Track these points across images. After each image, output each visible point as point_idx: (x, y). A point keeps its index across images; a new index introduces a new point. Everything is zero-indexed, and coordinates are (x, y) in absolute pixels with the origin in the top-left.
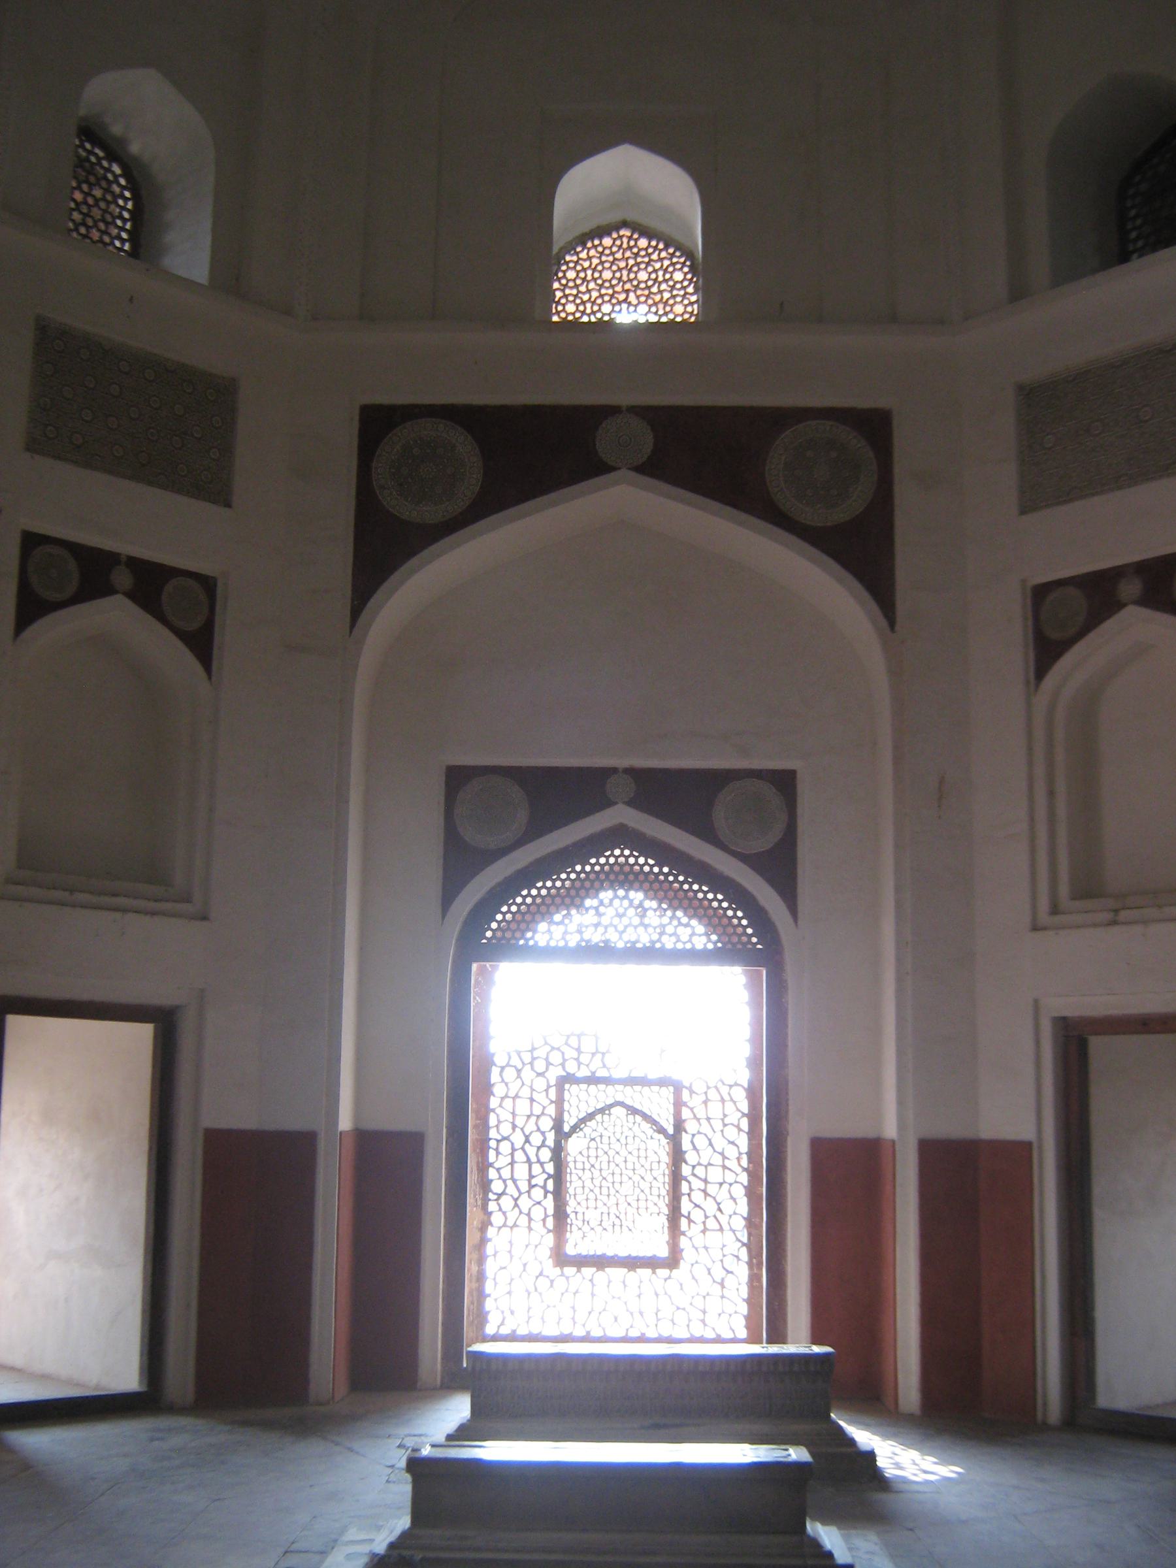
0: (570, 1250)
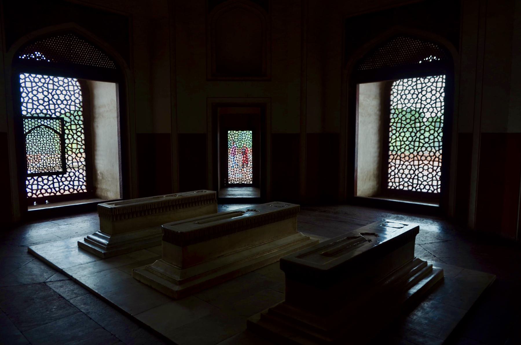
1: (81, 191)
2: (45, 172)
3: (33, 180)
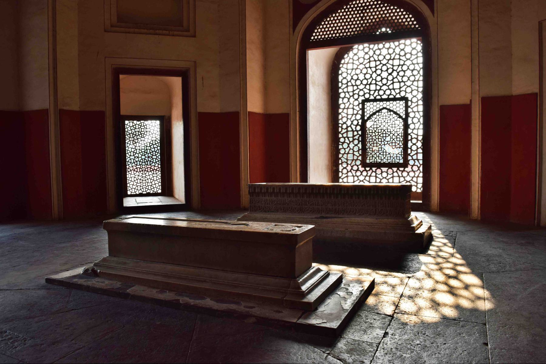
0: (368, 161)
2: (384, 163)
3: (371, 171)
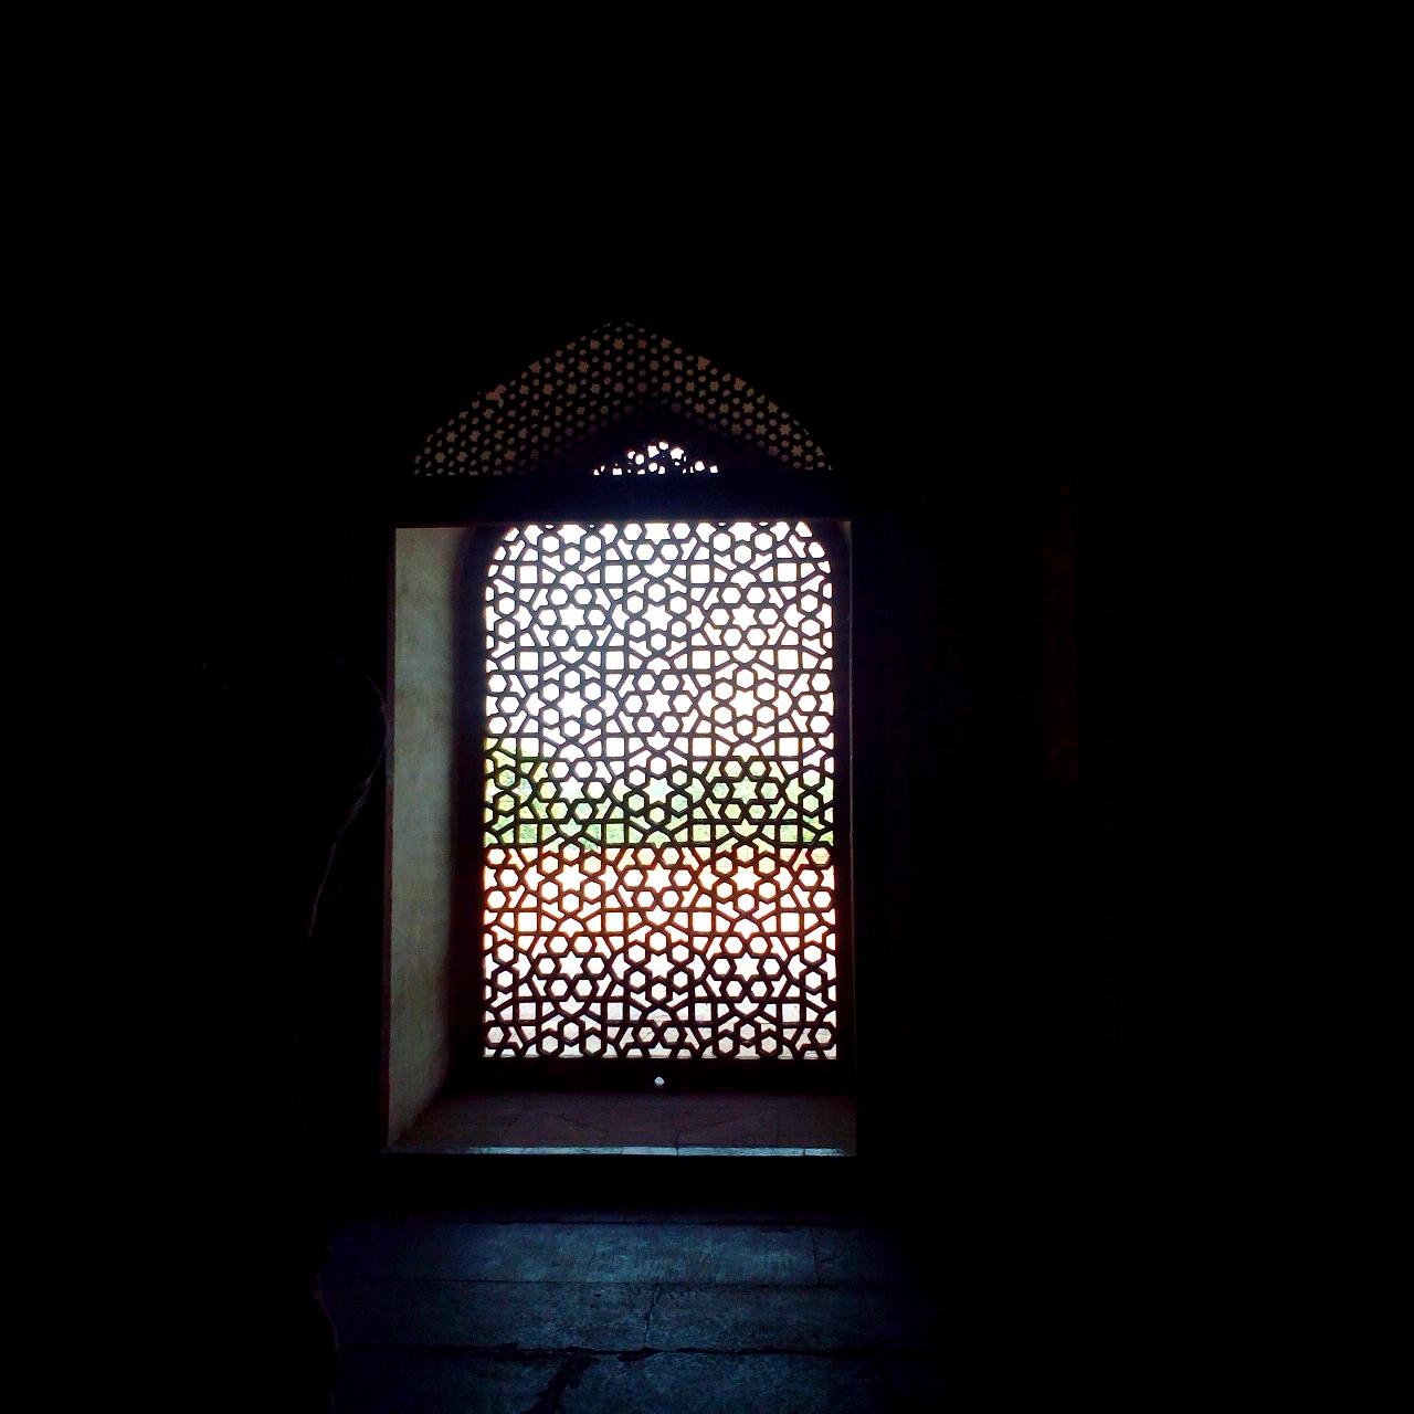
1: (811, 1055)
